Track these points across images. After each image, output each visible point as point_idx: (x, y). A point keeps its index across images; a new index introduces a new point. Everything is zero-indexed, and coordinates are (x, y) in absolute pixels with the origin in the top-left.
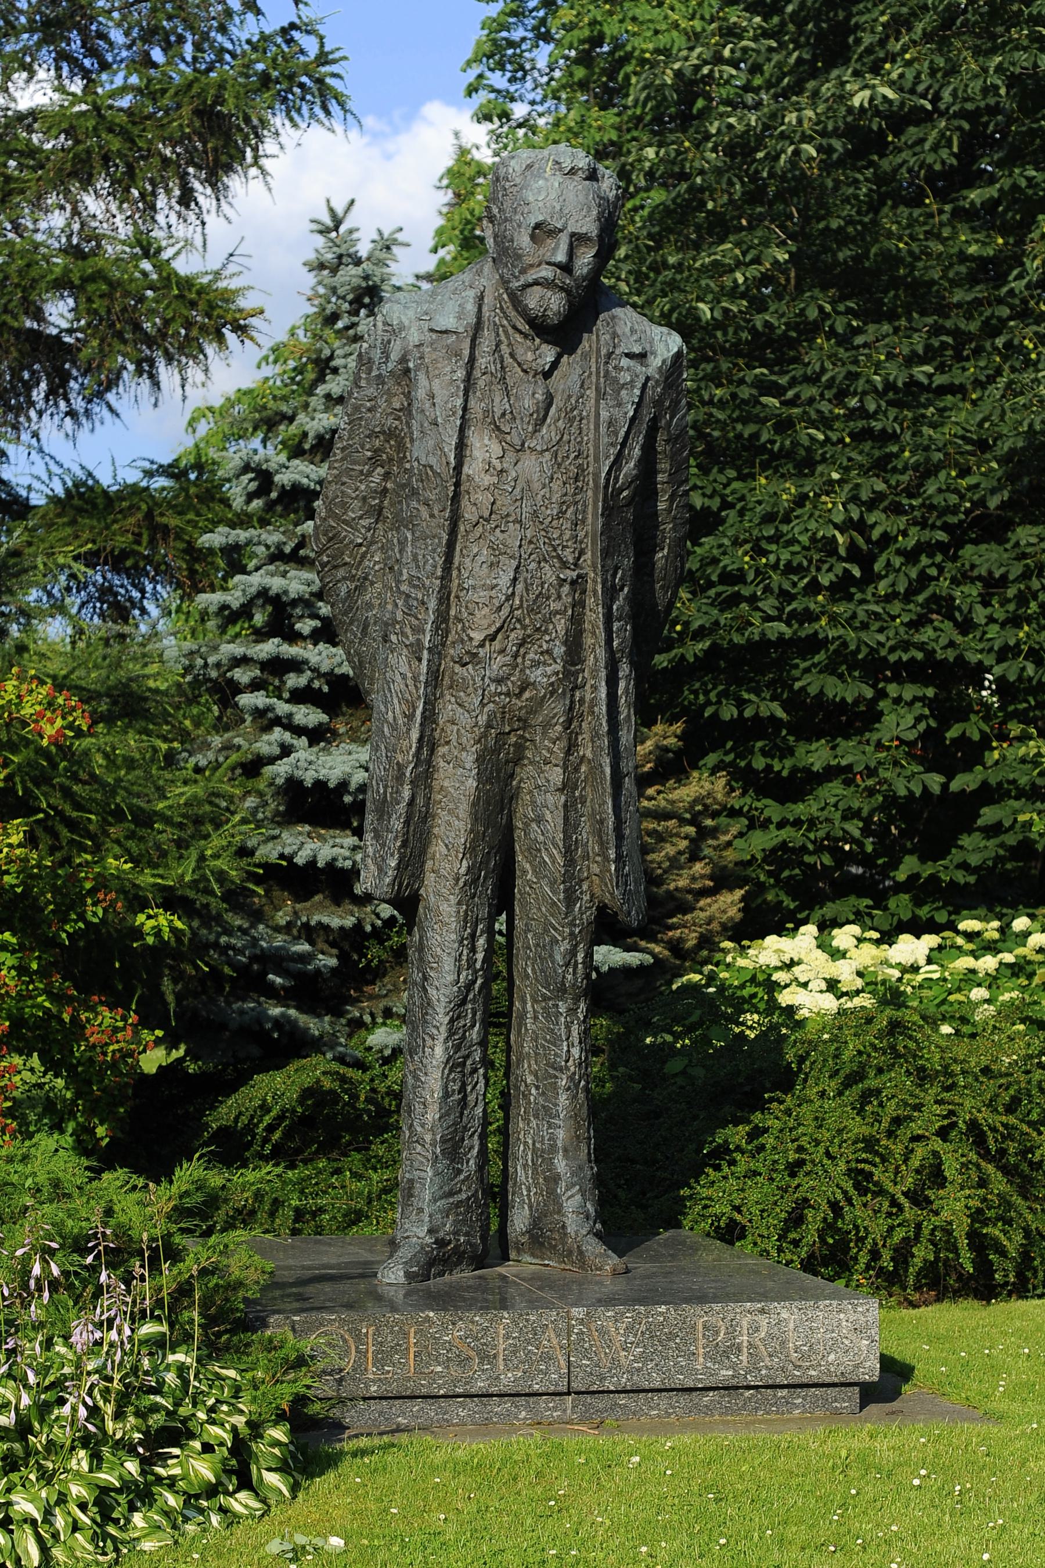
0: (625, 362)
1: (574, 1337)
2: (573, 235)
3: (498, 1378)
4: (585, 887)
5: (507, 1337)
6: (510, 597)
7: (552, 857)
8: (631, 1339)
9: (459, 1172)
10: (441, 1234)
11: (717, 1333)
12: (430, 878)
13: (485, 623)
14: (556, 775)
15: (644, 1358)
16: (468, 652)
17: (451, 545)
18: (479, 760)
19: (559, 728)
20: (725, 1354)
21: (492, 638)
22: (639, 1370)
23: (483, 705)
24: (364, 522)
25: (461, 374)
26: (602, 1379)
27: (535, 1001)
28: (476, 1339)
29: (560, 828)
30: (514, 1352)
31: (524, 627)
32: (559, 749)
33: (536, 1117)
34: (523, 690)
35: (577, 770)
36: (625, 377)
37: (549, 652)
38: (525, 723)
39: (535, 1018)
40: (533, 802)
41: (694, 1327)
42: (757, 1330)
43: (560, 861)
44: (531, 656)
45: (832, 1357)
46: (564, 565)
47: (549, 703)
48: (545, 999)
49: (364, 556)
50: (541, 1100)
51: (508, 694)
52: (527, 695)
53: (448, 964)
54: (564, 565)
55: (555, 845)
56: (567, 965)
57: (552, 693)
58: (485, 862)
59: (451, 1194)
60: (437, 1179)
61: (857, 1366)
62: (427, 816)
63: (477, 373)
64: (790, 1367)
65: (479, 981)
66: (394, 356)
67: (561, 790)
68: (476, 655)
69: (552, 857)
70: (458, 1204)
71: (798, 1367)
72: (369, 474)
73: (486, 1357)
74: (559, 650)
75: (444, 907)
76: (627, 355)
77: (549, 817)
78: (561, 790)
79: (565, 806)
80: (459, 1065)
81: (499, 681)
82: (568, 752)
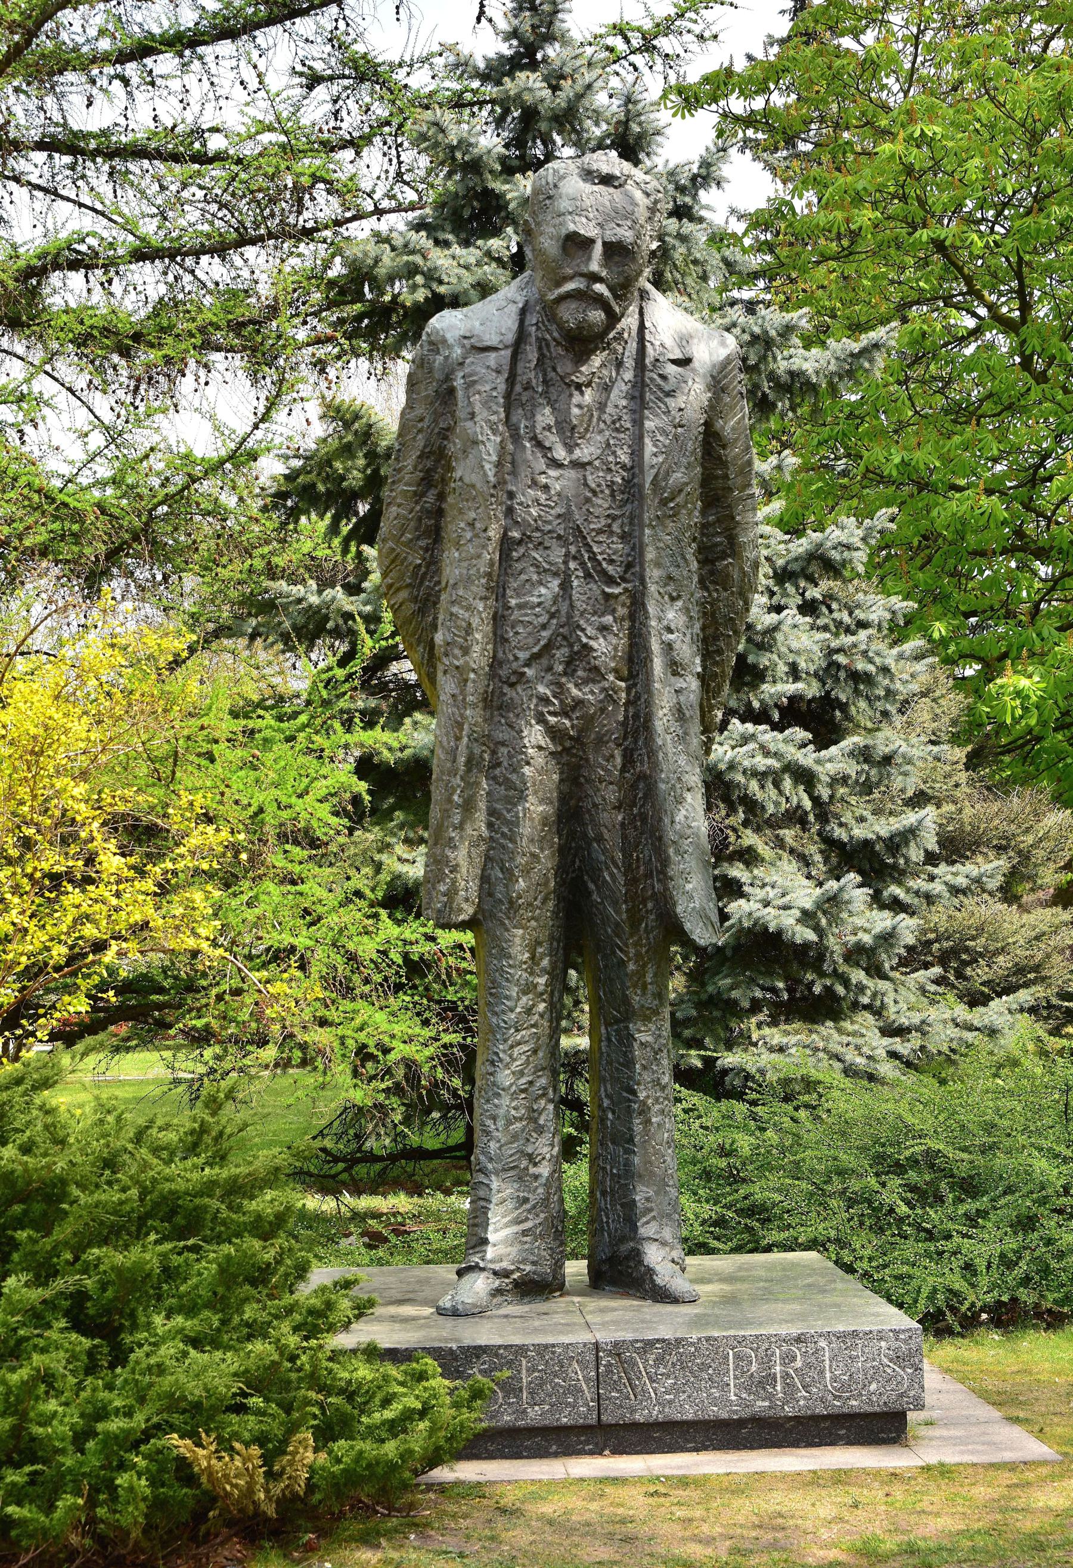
0: (671, 369)
1: (602, 1369)
3: (524, 1411)
4: (650, 905)
5: (531, 1370)
7: (612, 875)
8: (662, 1370)
10: (505, 1265)
13: (531, 640)
14: (611, 794)
15: (676, 1390)
16: (515, 672)
22: (670, 1402)
24: (422, 543)
26: (633, 1411)
30: (541, 1385)
31: (571, 646)
35: (634, 787)
39: (609, 1040)
41: (726, 1357)
43: (621, 880)
44: (580, 673)
45: (873, 1387)
46: (611, 581)
55: (617, 867)
61: (901, 1395)
63: (518, 388)
64: (830, 1397)
65: (542, 1006)
66: (438, 375)
67: (618, 808)
68: (523, 674)
69: (612, 875)
71: (835, 1397)
72: (423, 494)
73: (510, 1388)
76: (674, 362)
79: (622, 824)
80: (523, 1091)
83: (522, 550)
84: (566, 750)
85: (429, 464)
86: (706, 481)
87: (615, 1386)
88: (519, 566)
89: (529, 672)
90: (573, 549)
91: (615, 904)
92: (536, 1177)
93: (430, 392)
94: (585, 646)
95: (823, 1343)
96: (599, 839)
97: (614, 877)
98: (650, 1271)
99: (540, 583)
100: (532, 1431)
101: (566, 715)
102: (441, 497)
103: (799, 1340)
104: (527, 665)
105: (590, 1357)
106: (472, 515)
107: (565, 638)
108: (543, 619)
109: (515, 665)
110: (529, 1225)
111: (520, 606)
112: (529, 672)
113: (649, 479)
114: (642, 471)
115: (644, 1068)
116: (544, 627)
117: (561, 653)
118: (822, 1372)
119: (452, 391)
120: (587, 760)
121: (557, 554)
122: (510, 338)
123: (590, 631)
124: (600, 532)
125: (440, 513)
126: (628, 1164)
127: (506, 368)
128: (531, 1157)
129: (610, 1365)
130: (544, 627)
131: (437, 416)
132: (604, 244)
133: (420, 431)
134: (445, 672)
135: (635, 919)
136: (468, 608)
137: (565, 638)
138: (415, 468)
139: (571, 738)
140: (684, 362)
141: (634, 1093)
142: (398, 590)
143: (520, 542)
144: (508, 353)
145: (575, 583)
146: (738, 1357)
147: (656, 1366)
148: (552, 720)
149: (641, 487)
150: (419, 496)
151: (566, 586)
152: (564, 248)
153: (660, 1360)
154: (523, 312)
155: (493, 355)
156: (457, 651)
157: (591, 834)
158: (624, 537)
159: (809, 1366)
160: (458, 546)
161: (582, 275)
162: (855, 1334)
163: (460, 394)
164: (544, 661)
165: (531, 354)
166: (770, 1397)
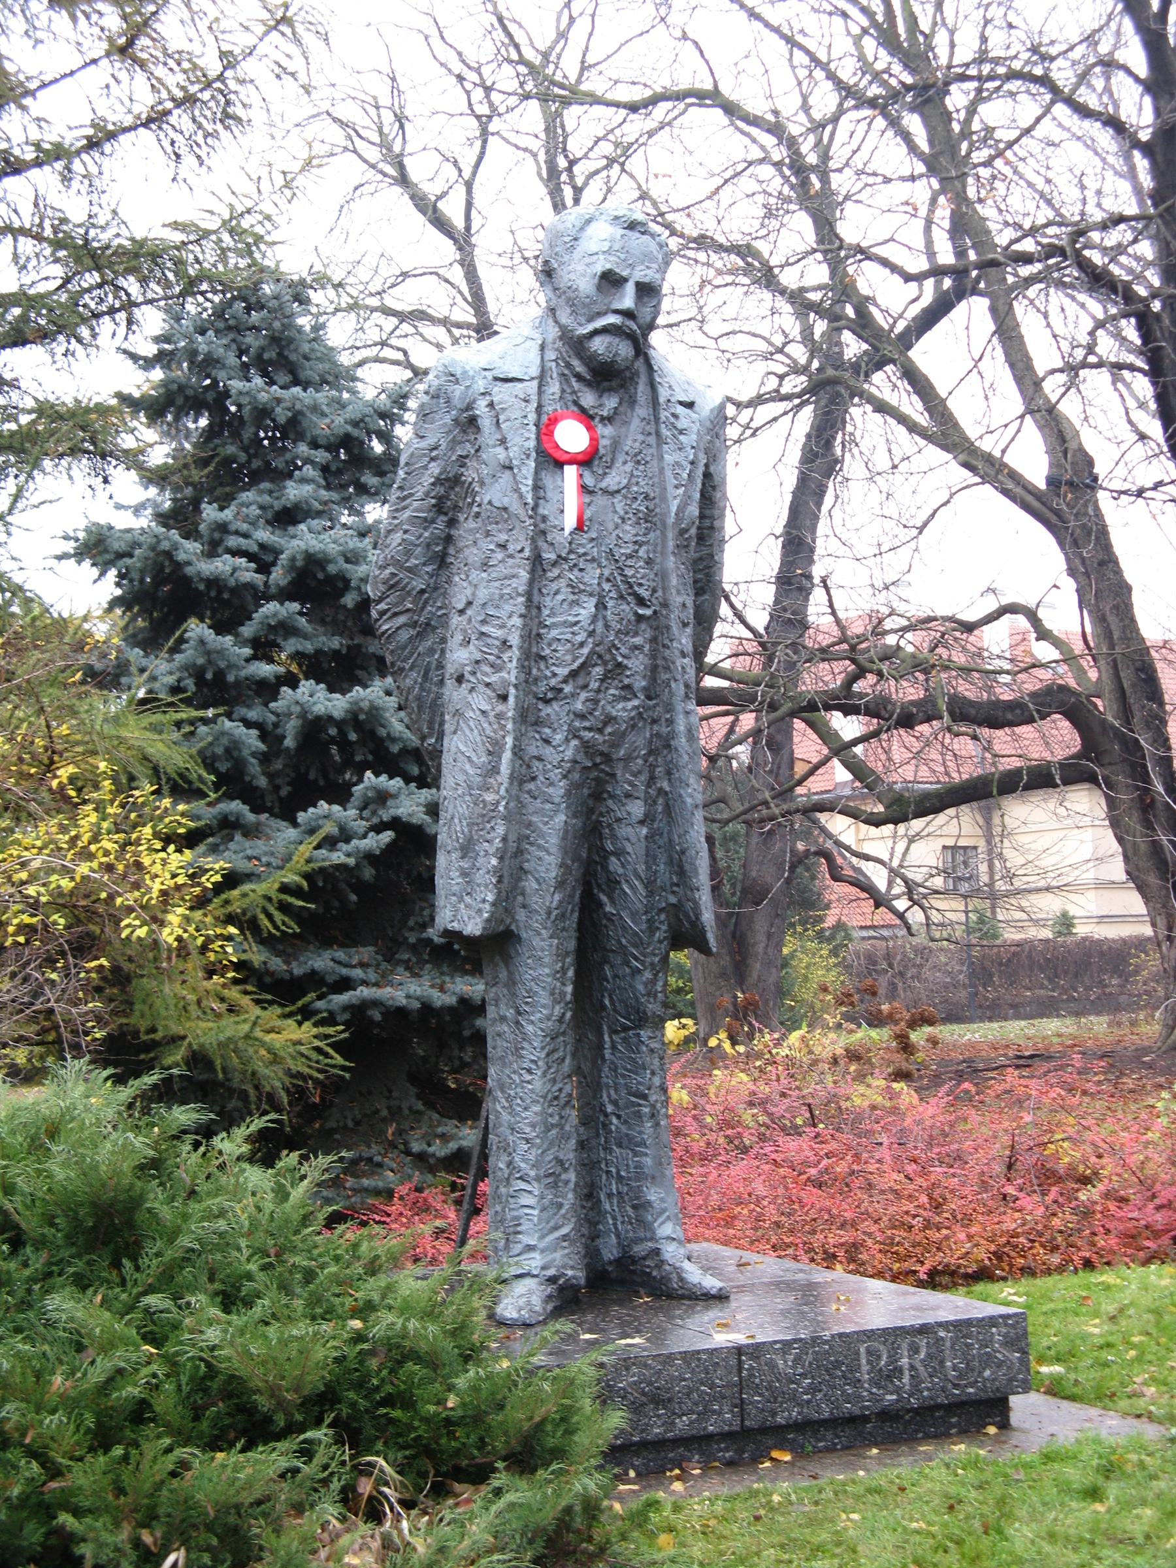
0: (680, 410)
2: (638, 284)
6: (591, 634)
7: (633, 888)
9: (561, 1206)
11: (879, 1357)
12: (521, 915)
13: (569, 658)
14: (637, 809)
15: (813, 1389)
17: (531, 582)
18: (568, 793)
19: (640, 761)
20: (889, 1377)
21: (574, 674)
22: (808, 1402)
23: (567, 740)
24: (429, 569)
25: (532, 417)
26: (774, 1414)
27: (613, 1032)
28: (650, 1383)
29: (642, 859)
31: (605, 663)
32: (641, 782)
33: (620, 1146)
34: (605, 724)
36: (682, 423)
37: (628, 687)
38: (607, 758)
40: (614, 837)
41: (857, 1353)
42: (917, 1351)
45: (987, 1373)
47: (631, 737)
48: (625, 1029)
49: (426, 602)
50: (624, 1129)
51: (590, 729)
52: (609, 730)
53: (544, 998)
54: (641, 602)
55: (638, 877)
56: (648, 994)
57: (633, 727)
58: (571, 896)
59: (556, 1228)
60: (545, 1215)
62: (519, 852)
67: (642, 822)
68: (561, 690)
69: (632, 887)
70: (565, 1238)
71: (956, 1386)
72: (433, 521)
74: (640, 683)
75: (536, 942)
77: (629, 849)
78: (642, 822)
81: (582, 716)
82: (648, 786)
83: (556, 572)
84: (596, 765)
85: (440, 490)
86: (702, 516)
87: (757, 1390)
88: (554, 586)
89: (568, 689)
90: (607, 572)
91: (634, 915)
92: (567, 1182)
93: (448, 419)
94: (619, 665)
95: (942, 1334)
96: (619, 853)
97: (634, 892)
98: (678, 1271)
99: (576, 603)
100: (678, 1442)
101: (600, 731)
102: (452, 523)
103: (923, 1330)
104: (565, 681)
105: (733, 1362)
106: (503, 537)
107: (600, 656)
108: (579, 638)
109: (553, 682)
110: (565, 1230)
111: (554, 625)
112: (568, 689)
113: (674, 509)
114: (664, 499)
115: (653, 1073)
116: (582, 645)
117: (598, 671)
118: (942, 1363)
119: (473, 421)
120: (613, 775)
121: (592, 575)
122: (534, 371)
123: (623, 650)
124: (630, 556)
125: (448, 539)
126: (638, 1166)
127: (534, 398)
128: (560, 1162)
129: (752, 1368)
130: (582, 645)
131: (454, 443)
132: (638, 284)
133: (433, 459)
134: (472, 690)
135: (652, 929)
136: (503, 626)
137: (600, 656)
138: (427, 494)
139: (602, 754)
140: (690, 405)
141: (644, 1097)
142: (396, 614)
143: (554, 564)
144: (535, 383)
145: (610, 604)
146: (869, 1352)
147: (794, 1367)
148: (588, 735)
149: (665, 515)
150: (427, 522)
151: (601, 606)
152: (599, 288)
153: (798, 1360)
154: (542, 347)
155: (519, 385)
156: (487, 669)
157: (609, 846)
158: (649, 562)
159: (929, 1356)
160: (485, 566)
161: (617, 312)
162: (968, 1323)
163: (486, 423)
164: (581, 681)
165: (554, 388)
166: (898, 1390)
